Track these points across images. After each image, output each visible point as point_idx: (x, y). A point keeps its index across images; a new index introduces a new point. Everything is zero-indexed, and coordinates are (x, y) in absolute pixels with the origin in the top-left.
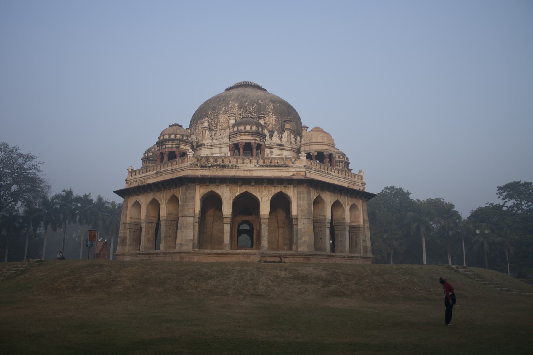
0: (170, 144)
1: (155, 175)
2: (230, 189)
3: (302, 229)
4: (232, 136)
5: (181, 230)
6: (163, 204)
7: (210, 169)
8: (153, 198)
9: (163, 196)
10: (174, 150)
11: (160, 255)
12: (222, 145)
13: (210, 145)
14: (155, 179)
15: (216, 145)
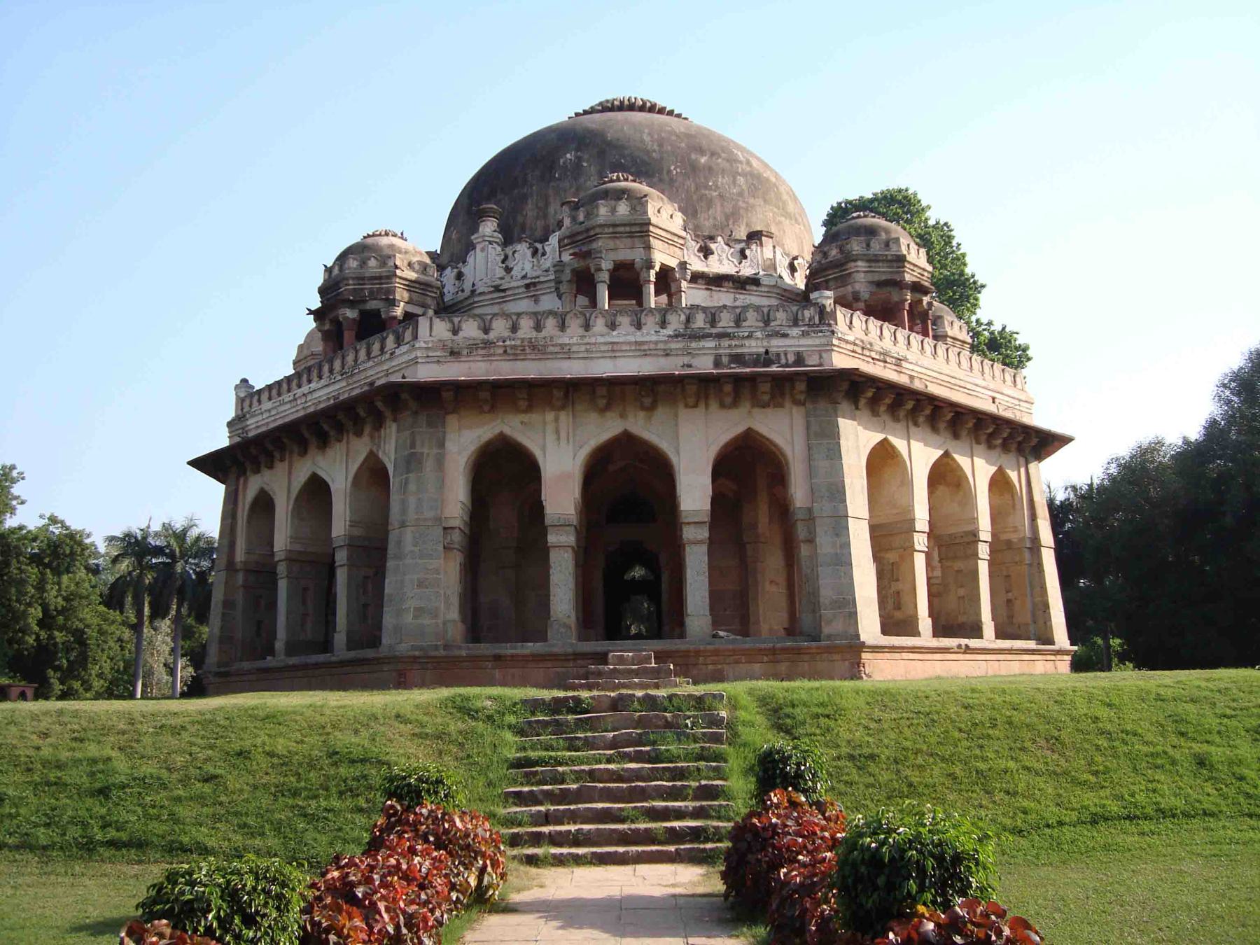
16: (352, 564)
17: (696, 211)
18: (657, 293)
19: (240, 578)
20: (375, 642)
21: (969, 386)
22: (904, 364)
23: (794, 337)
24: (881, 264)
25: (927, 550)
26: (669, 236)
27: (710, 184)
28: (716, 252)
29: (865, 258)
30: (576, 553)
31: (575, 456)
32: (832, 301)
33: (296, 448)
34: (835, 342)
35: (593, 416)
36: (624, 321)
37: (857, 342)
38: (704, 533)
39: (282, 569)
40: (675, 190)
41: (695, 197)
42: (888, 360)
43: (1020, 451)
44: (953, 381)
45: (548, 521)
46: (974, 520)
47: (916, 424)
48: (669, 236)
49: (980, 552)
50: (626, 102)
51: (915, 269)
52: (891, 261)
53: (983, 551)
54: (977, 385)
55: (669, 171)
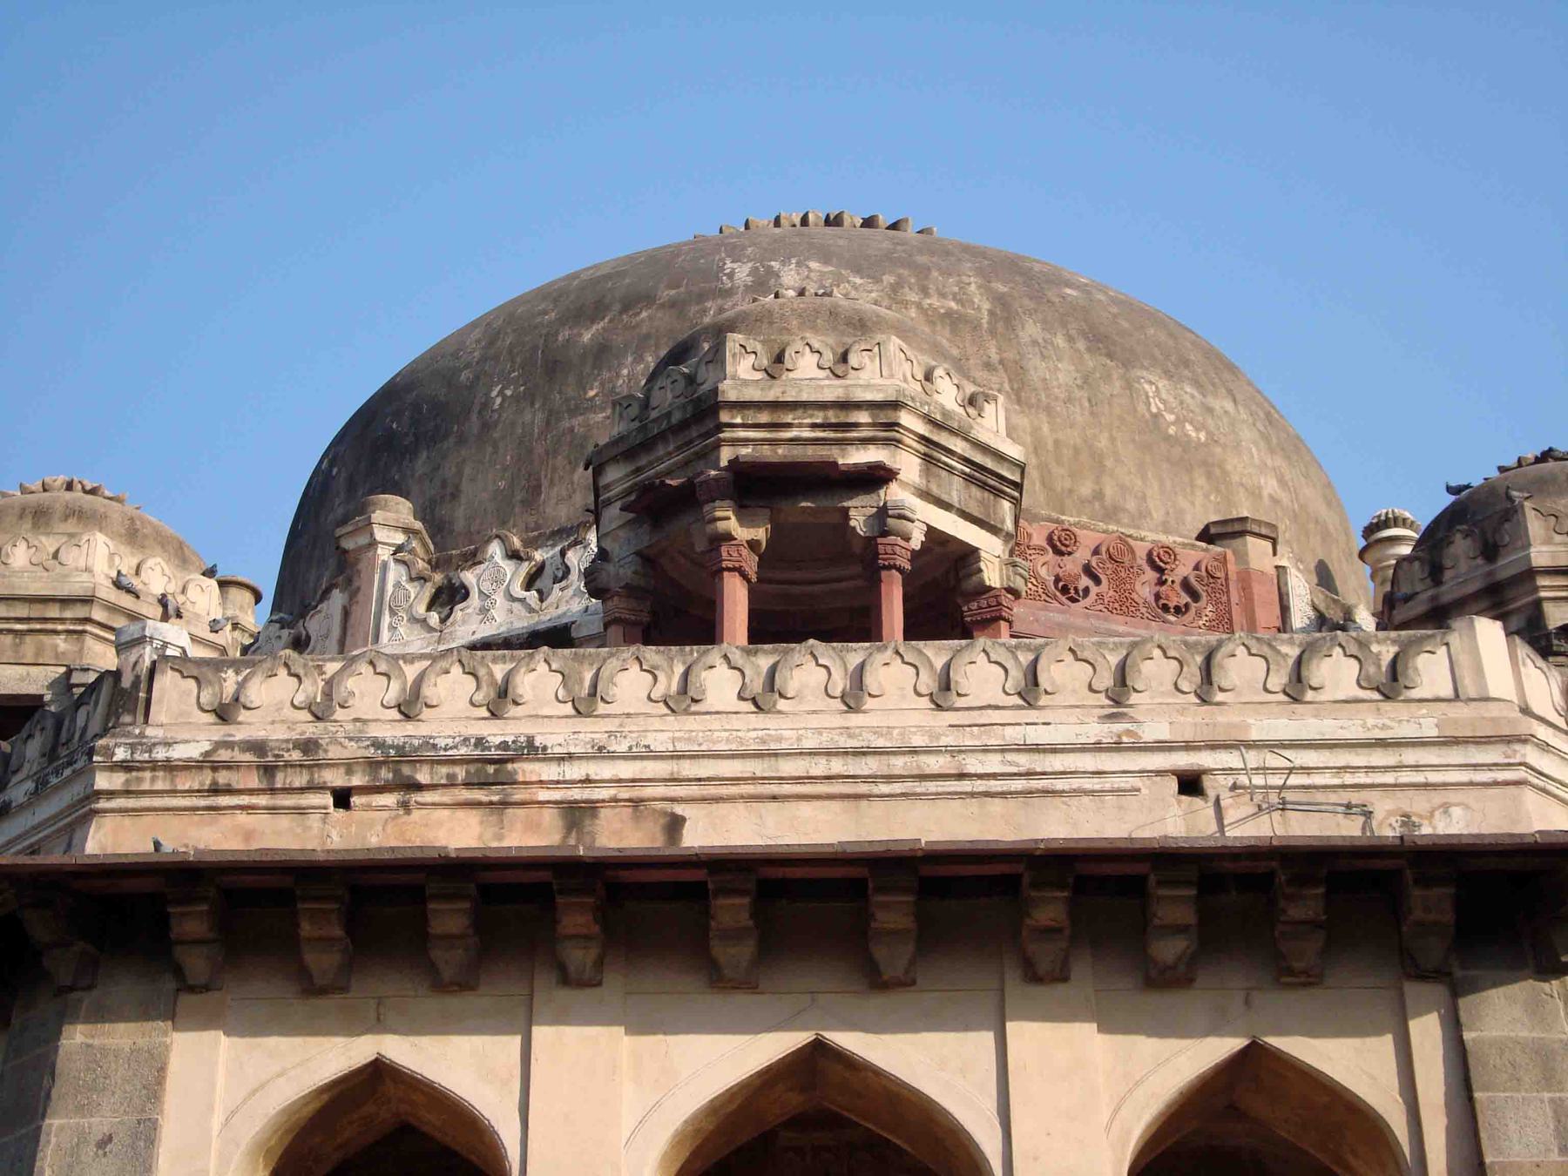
17: (536, 490)
21: (973, 764)
22: (528, 770)
23: (21, 807)
24: (661, 451)
26: (22, 611)
27: (591, 393)
28: (474, 594)
29: (615, 451)
34: (102, 781)
37: (224, 755)
40: (490, 449)
41: (539, 450)
42: (423, 777)
44: (869, 766)
48: (22, 611)
51: (789, 418)
52: (684, 425)
54: (1037, 749)
55: (486, 404)
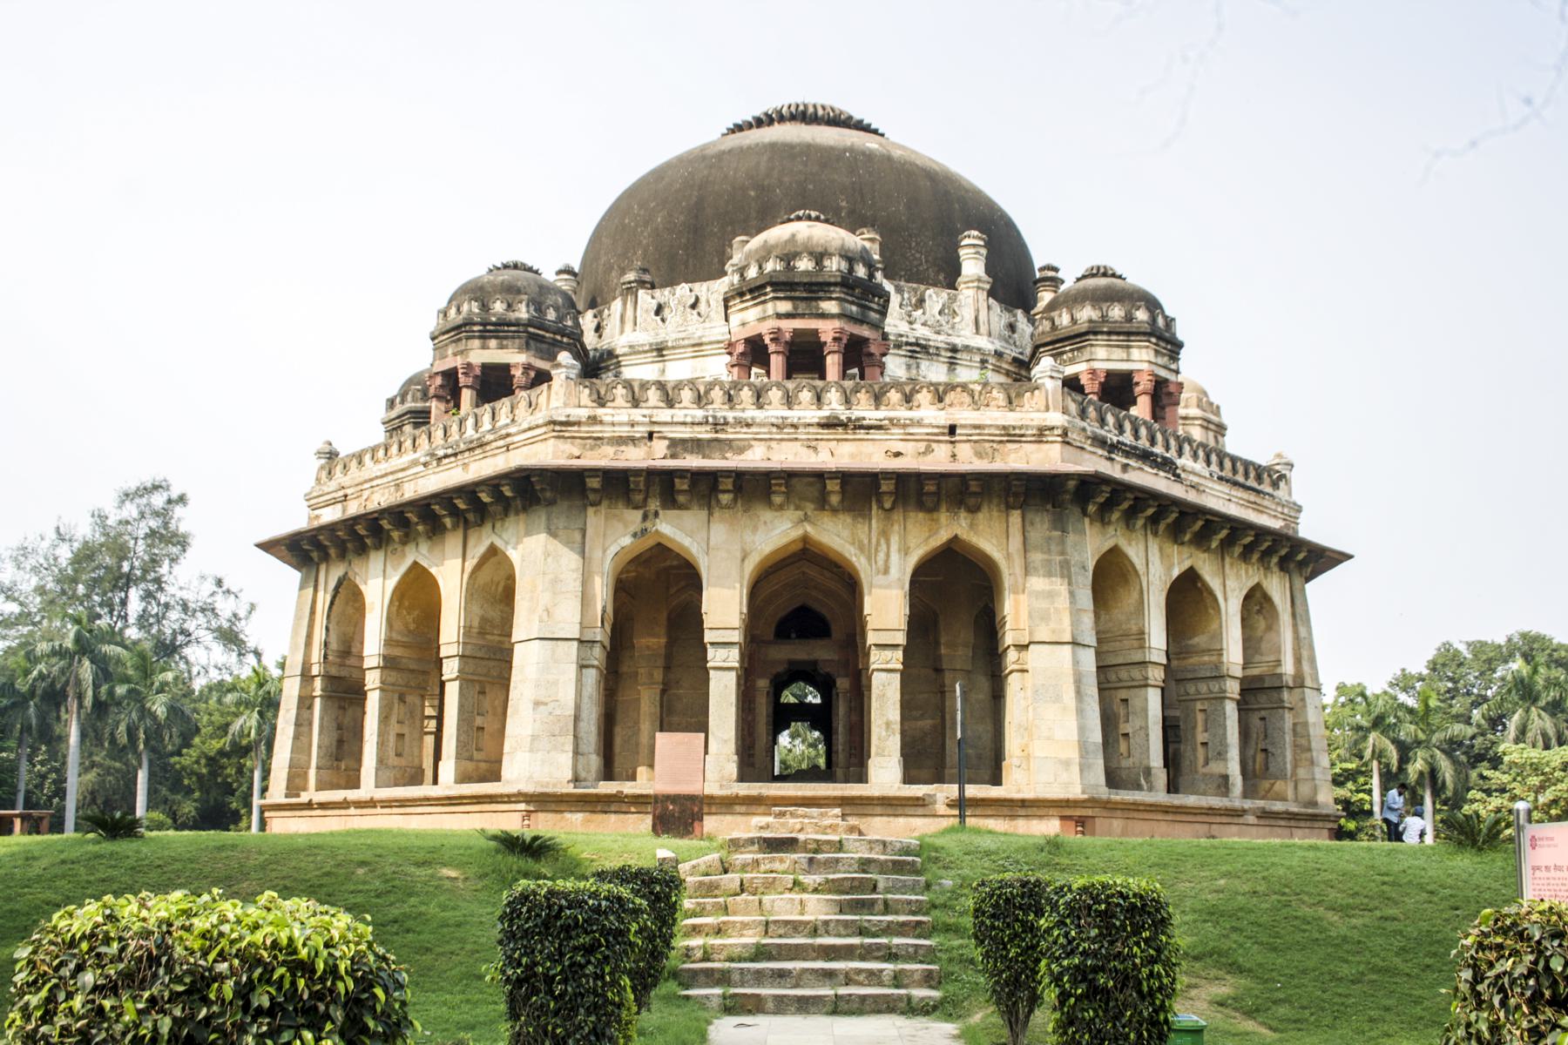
0: (858, 305)
1: (811, 430)
2: (1161, 549)
3: (1314, 724)
4: (1105, 337)
5: (1058, 699)
6: (886, 571)
7: (1113, 456)
8: (796, 533)
9: (885, 534)
10: (865, 332)
11: (920, 811)
12: (958, 356)
13: (907, 344)
14: (815, 448)
15: (937, 348)
16: (464, 678)
18: (846, 365)
19: (318, 683)
20: (496, 777)
25: (1162, 684)
30: (738, 678)
31: (743, 560)
32: (1060, 383)
33: (395, 535)
35: (767, 515)
36: (806, 396)
38: (896, 659)
39: (372, 680)
43: (1283, 565)
45: (708, 637)
46: (1220, 652)
47: (1155, 534)
49: (1229, 690)
50: (811, 110)
53: (1233, 688)
